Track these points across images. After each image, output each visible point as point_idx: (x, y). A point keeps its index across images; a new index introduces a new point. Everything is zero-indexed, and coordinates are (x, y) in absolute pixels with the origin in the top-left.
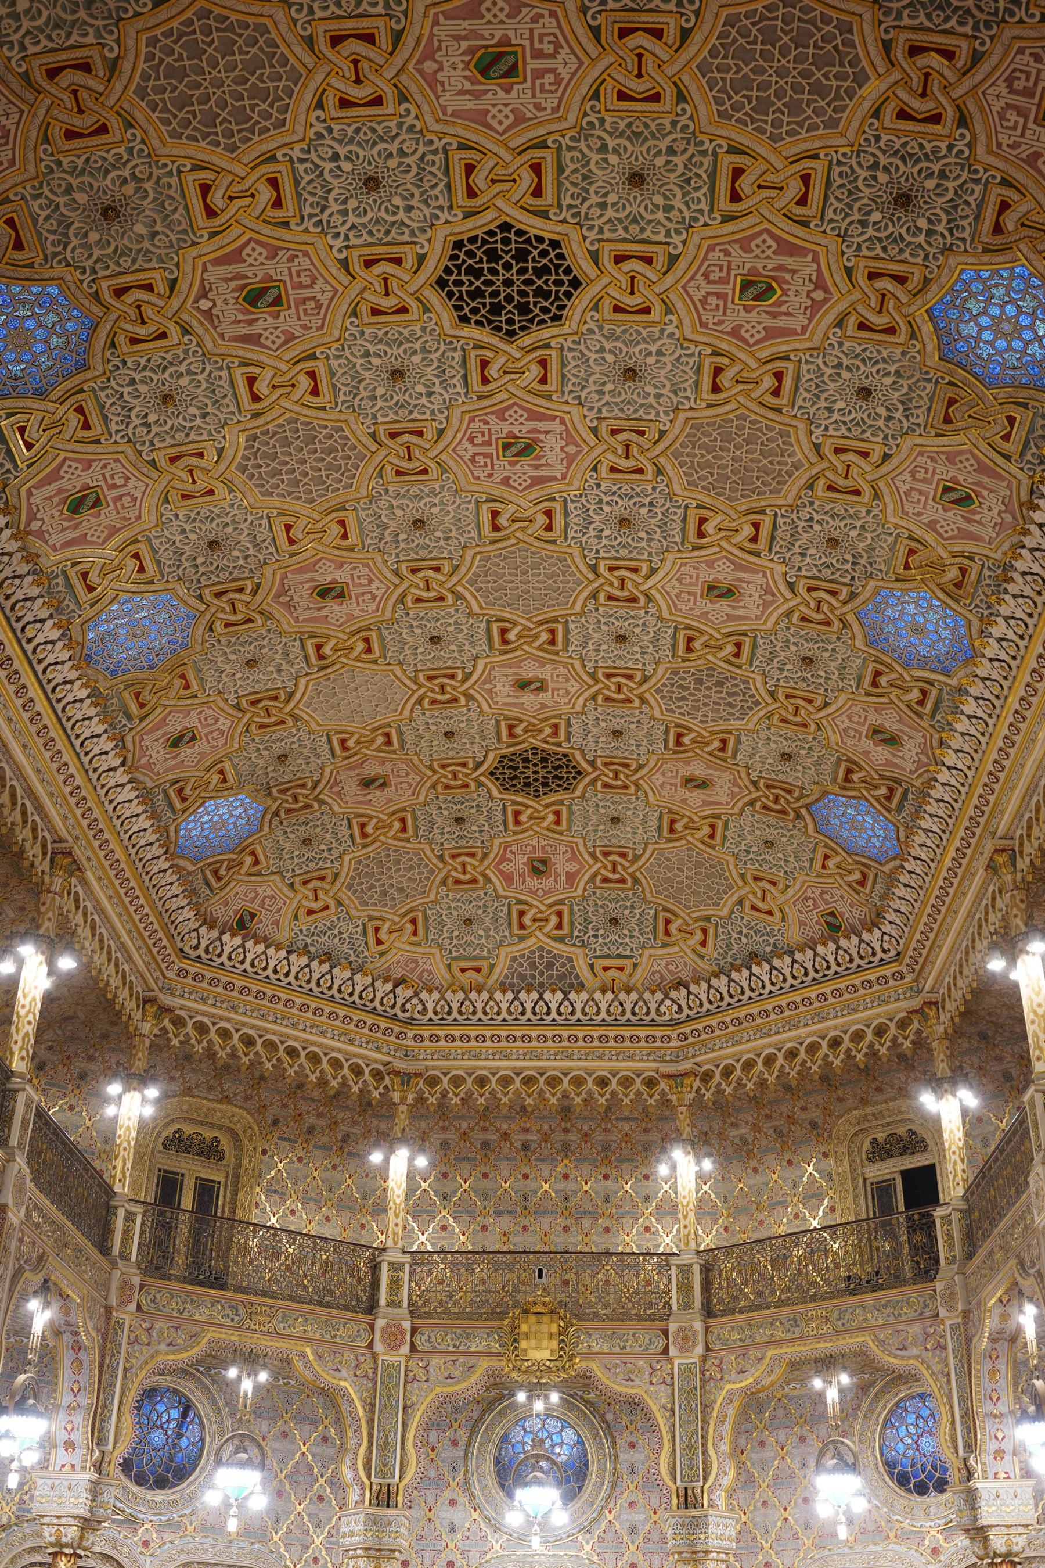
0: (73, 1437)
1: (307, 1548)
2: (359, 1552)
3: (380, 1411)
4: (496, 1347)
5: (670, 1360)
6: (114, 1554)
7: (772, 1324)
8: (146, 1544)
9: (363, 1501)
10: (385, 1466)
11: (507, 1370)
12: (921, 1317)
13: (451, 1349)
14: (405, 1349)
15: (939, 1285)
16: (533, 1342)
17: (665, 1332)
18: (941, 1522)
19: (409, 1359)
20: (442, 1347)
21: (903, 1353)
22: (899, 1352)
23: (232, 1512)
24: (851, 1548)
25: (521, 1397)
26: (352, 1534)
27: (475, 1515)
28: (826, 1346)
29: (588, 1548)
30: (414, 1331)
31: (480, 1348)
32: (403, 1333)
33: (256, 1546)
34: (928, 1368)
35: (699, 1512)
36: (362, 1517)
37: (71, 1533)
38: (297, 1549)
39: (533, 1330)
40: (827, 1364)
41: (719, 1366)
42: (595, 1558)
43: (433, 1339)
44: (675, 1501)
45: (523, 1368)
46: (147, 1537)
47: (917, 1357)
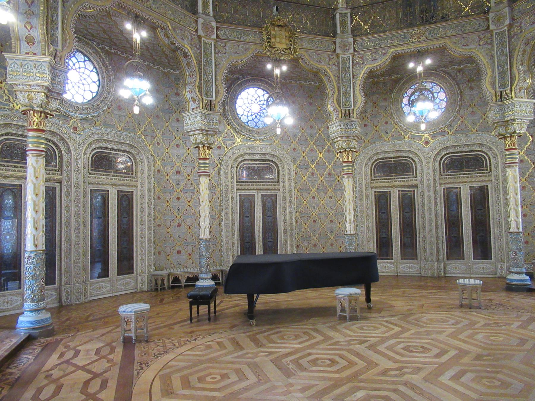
0: (32, 33)
1: (153, 138)
2: (197, 132)
3: (204, 65)
4: (258, 41)
5: (338, 55)
6: (58, 131)
7: (391, 38)
8: (75, 129)
9: (199, 107)
10: (207, 92)
11: (265, 51)
12: (477, 31)
13: (236, 39)
14: (214, 37)
15: (491, 15)
16: (278, 40)
17: (335, 43)
18: (431, 131)
19: (216, 42)
20: (232, 38)
21: (467, 47)
22: (464, 47)
23: (135, 103)
24: (387, 142)
25: (269, 66)
26: (193, 123)
27: (229, 127)
28: (422, 46)
29: (277, 142)
30: (217, 28)
31: (251, 40)
32: (212, 28)
33: (132, 134)
34: (481, 53)
35: (351, 120)
36: (200, 114)
37: (40, 97)
38: (149, 138)
39: (278, 33)
40: (419, 55)
41: (362, 58)
42: (280, 146)
43: (227, 33)
44: (340, 115)
45: (273, 51)
46: (75, 125)
47: (473, 48)
